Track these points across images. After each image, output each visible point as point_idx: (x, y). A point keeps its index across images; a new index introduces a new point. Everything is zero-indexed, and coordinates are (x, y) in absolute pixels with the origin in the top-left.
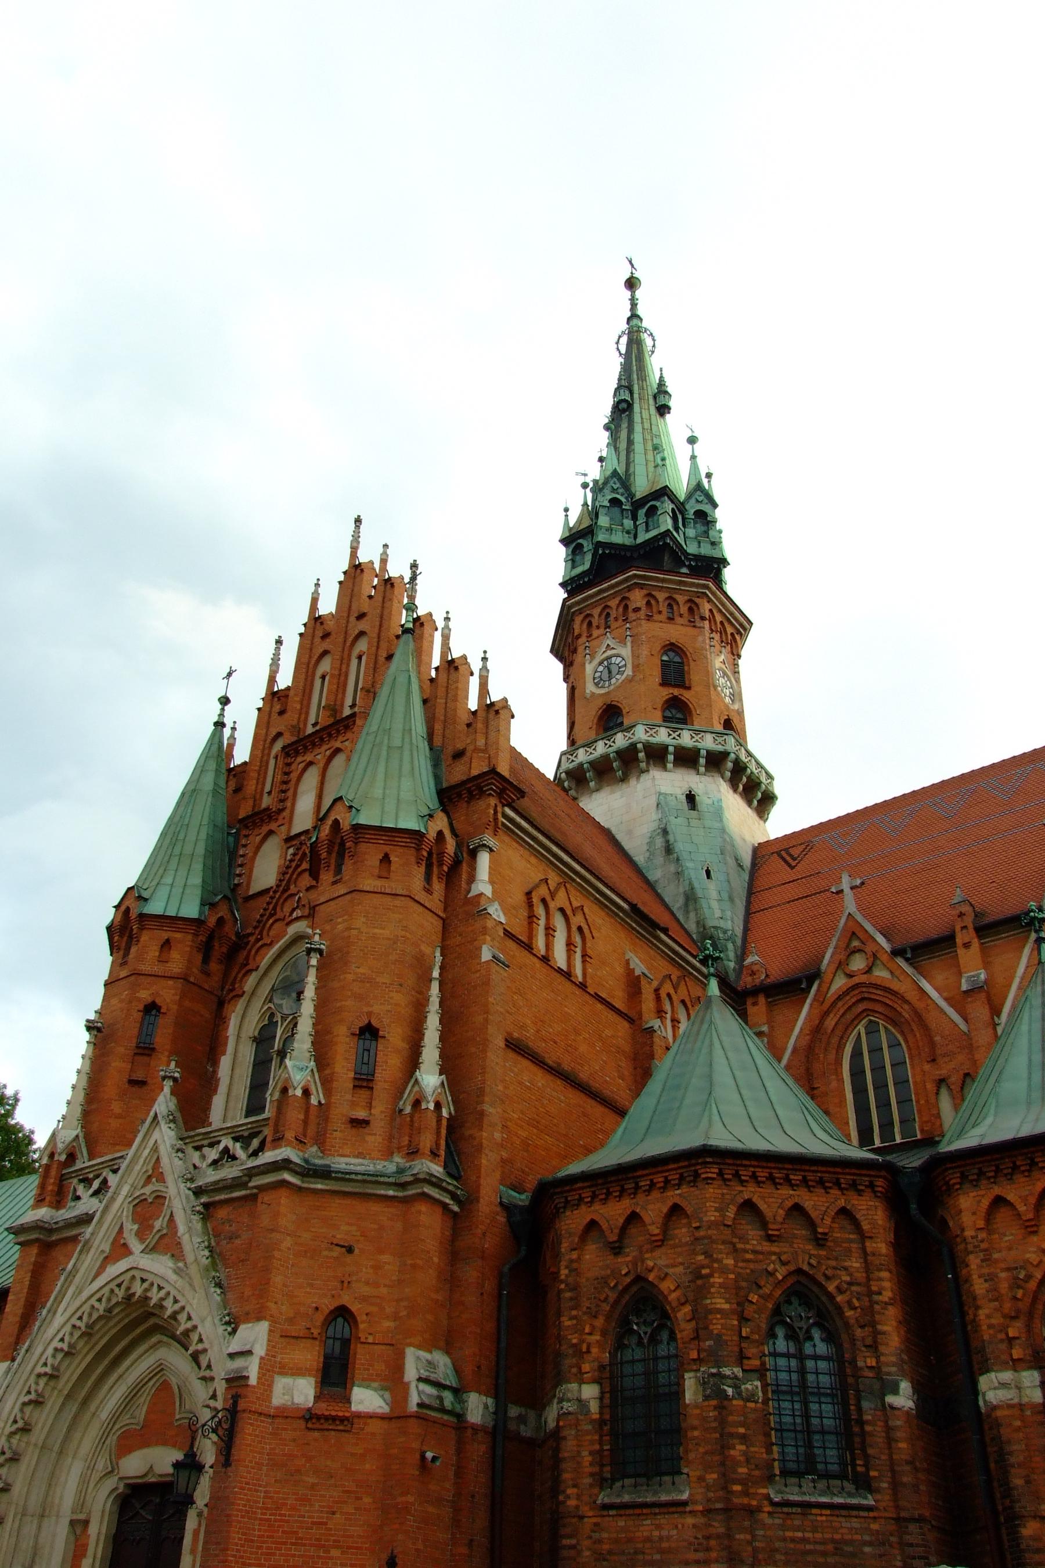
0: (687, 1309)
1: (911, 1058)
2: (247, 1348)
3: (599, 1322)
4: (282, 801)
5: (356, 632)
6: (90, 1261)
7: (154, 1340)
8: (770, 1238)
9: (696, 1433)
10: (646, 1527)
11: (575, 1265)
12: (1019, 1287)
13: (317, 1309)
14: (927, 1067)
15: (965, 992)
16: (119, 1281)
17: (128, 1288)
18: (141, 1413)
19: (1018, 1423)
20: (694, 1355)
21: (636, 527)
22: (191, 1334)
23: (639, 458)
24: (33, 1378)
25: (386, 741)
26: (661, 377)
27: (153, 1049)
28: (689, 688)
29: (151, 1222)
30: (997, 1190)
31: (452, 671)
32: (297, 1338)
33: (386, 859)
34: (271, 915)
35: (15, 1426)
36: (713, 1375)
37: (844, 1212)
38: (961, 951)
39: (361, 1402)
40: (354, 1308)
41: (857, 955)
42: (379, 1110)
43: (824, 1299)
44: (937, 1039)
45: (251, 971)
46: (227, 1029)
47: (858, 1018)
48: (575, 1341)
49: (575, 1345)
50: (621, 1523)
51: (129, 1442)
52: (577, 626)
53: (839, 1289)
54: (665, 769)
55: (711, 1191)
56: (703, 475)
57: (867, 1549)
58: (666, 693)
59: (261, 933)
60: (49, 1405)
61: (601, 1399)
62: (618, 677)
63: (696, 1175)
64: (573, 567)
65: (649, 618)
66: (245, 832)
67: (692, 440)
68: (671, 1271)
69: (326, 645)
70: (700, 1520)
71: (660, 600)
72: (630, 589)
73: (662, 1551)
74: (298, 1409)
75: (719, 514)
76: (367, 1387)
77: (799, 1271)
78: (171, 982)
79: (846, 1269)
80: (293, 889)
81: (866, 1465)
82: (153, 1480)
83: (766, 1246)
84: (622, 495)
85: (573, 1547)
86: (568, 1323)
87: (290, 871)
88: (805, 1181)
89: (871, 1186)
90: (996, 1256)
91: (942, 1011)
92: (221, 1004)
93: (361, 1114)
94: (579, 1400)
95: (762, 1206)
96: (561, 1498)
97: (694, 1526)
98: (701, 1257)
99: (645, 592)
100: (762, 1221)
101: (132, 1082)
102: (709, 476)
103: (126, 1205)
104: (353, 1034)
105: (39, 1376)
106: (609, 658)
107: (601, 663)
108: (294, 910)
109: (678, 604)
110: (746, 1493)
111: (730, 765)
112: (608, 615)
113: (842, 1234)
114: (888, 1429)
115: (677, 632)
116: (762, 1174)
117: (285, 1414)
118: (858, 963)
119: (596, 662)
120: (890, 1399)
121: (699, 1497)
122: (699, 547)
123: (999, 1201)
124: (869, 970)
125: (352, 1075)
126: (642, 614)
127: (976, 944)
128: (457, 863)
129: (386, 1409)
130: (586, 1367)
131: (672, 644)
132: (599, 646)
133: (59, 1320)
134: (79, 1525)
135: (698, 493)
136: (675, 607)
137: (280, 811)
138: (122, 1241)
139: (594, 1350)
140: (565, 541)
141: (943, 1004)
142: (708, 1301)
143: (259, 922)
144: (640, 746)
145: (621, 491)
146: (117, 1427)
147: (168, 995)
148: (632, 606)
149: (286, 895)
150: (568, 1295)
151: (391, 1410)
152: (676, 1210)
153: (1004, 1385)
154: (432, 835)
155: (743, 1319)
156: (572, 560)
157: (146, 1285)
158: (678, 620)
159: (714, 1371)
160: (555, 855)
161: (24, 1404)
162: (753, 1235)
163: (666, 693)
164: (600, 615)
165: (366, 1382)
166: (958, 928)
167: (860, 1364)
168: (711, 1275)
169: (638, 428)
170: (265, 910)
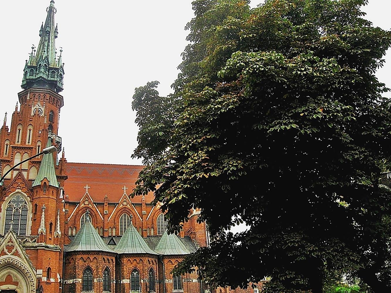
20: (96, 277)
67: (61, 51)
72: (47, 93)
83: (104, 263)
102: (63, 64)
139: (81, 275)
145: (47, 62)
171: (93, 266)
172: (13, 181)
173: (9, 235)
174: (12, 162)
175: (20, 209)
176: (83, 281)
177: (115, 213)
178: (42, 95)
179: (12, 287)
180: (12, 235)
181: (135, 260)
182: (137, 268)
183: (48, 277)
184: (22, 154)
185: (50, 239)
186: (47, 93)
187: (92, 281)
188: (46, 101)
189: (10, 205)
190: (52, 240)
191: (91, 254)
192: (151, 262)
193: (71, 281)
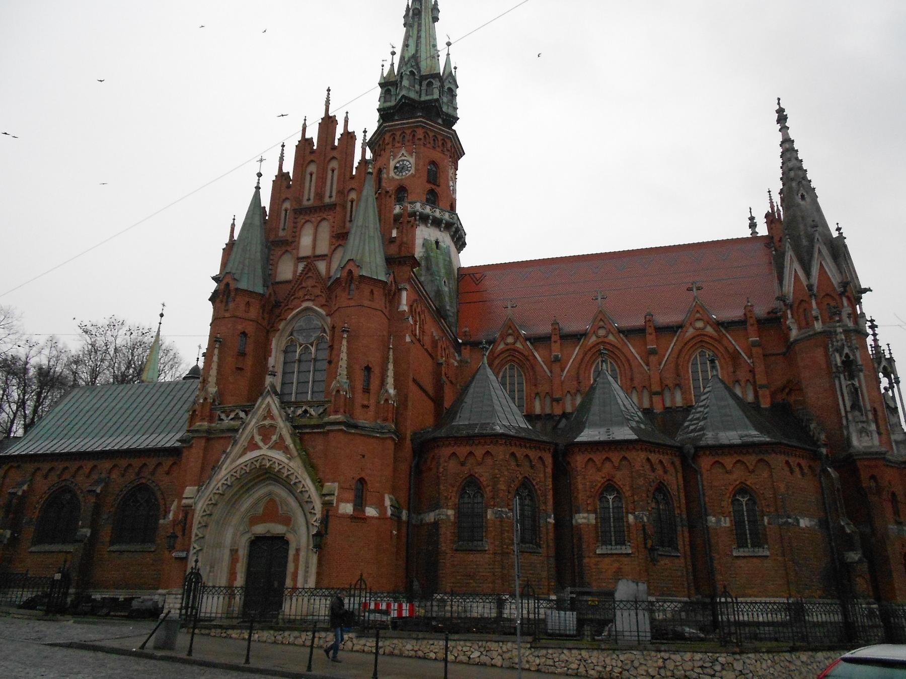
1: (526, 382)
2: (332, 492)
3: (455, 489)
4: (293, 237)
5: (331, 156)
6: (238, 449)
7: (268, 482)
8: (518, 465)
9: (491, 529)
10: (471, 557)
11: (446, 468)
12: (593, 488)
17: (261, 463)
19: (587, 529)
20: (492, 503)
23: (423, 47)
25: (367, 233)
28: (439, 186)
29: (269, 436)
30: (591, 456)
31: (388, 197)
33: (372, 292)
34: (293, 295)
35: (205, 514)
37: (540, 458)
38: (553, 344)
40: (366, 479)
41: (510, 336)
42: (372, 401)
44: (538, 377)
45: (282, 320)
52: (387, 137)
53: (536, 483)
54: (427, 226)
55: (502, 448)
56: (452, 67)
58: (429, 186)
62: (407, 172)
64: (385, 102)
65: (424, 145)
66: (273, 248)
67: (449, 44)
69: (312, 157)
70: (491, 556)
72: (417, 127)
73: (477, 565)
74: (348, 515)
75: (458, 91)
76: (371, 507)
77: (526, 477)
78: (251, 323)
80: (304, 285)
81: (540, 540)
83: (517, 468)
84: (415, 69)
87: (303, 275)
90: (587, 477)
92: (268, 332)
93: (366, 403)
94: (447, 515)
96: (439, 547)
102: (455, 68)
106: (403, 161)
107: (398, 162)
108: (305, 295)
110: (507, 548)
111: (454, 229)
113: (539, 465)
114: (547, 529)
116: (518, 443)
117: (344, 516)
118: (510, 340)
119: (396, 161)
120: (548, 520)
121: (491, 549)
122: (448, 109)
125: (362, 387)
128: (395, 294)
129: (377, 515)
130: (450, 504)
131: (433, 161)
132: (398, 153)
133: (223, 472)
134: (234, 552)
135: (450, 77)
136: (436, 141)
137: (292, 242)
139: (453, 498)
140: (381, 85)
141: (542, 363)
144: (418, 213)
145: (415, 67)
146: (249, 514)
147: (250, 329)
149: (300, 287)
151: (379, 514)
152: (488, 453)
153: (584, 518)
154: (389, 283)
155: (509, 492)
157: (271, 463)
160: (418, 288)
161: (208, 504)
162: (513, 463)
163: (429, 186)
164: (400, 136)
165: (370, 506)
167: (541, 508)
169: (423, 28)
171: (484, 474)
172: (295, 284)
173: (266, 402)
174: (295, 243)
175: (312, 346)
176: (459, 514)
177: (580, 357)
178: (408, 132)
179: (278, 529)
181: (607, 459)
182: (615, 482)
183: (359, 504)
184: (315, 224)
185: (365, 407)
186: (417, 127)
187: (483, 515)
188: (417, 142)
189: (292, 341)
190: (372, 408)
191: (476, 442)
192: (658, 467)
193: (430, 517)
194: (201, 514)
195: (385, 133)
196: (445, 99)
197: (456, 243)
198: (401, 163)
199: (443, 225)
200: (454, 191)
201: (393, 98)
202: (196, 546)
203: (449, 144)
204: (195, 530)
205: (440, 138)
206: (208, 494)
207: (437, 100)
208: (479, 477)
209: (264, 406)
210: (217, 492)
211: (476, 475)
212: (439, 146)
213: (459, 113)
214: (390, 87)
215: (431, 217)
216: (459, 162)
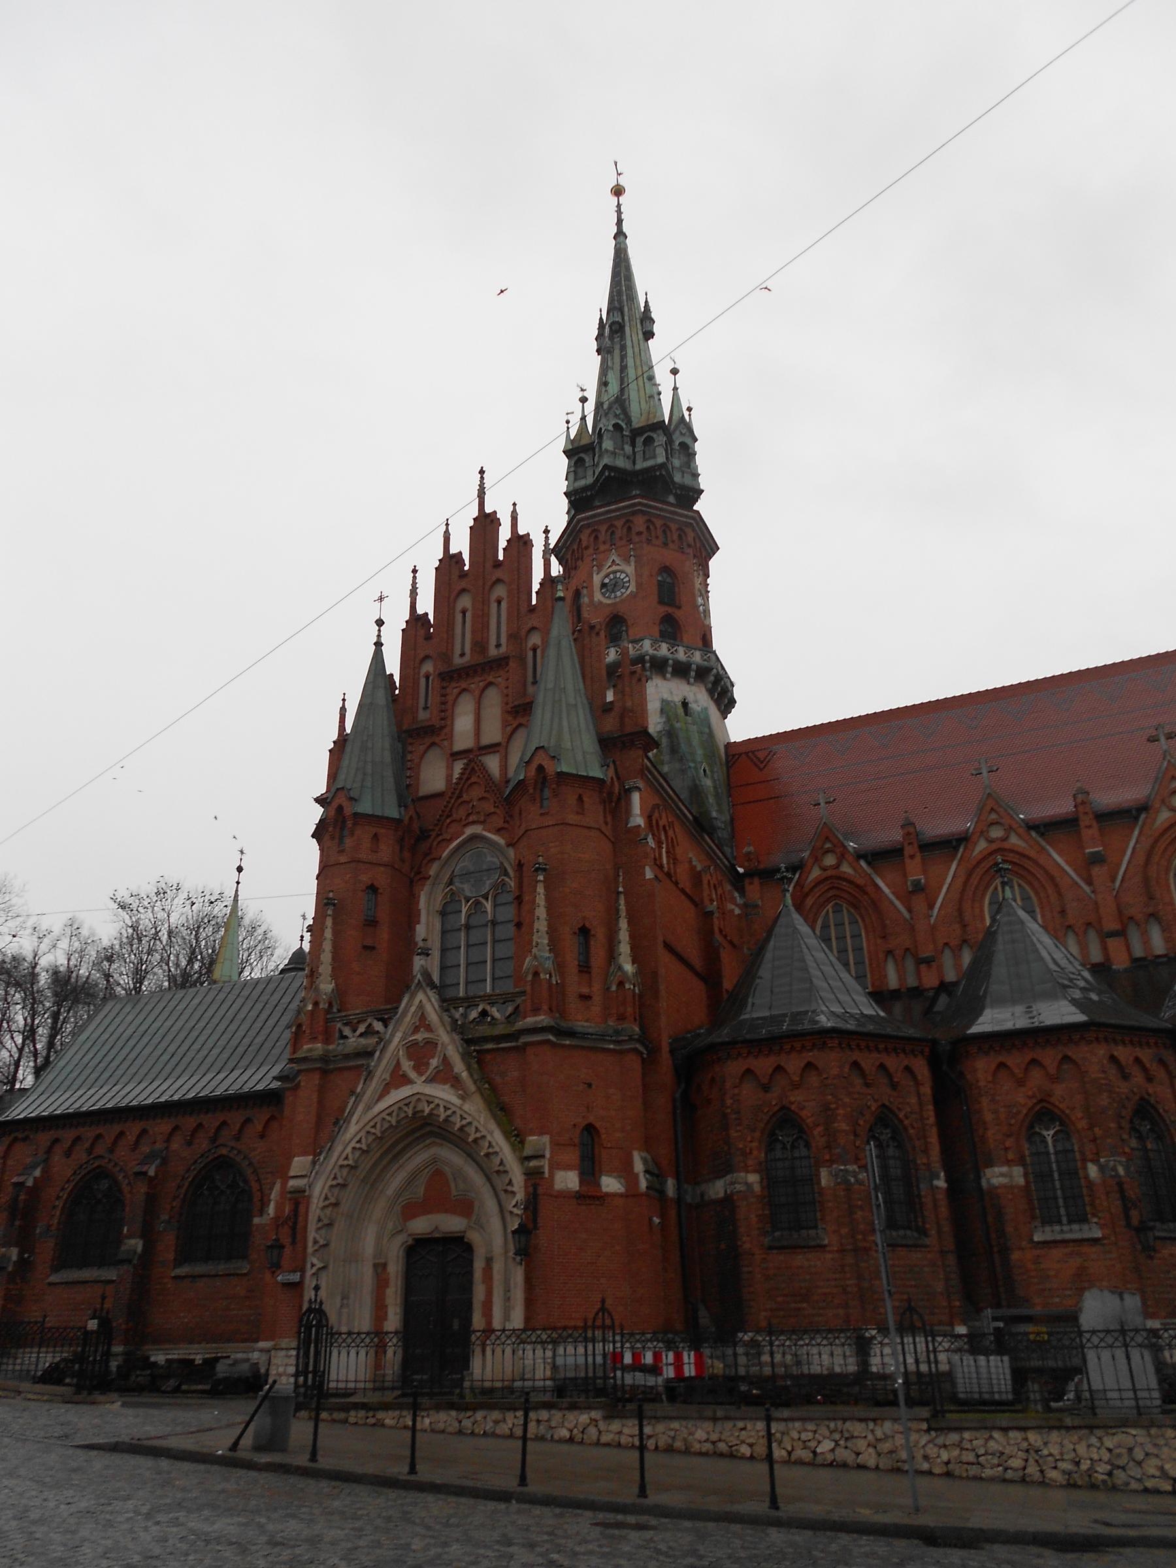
0: (820, 1129)
2: (541, 1153)
3: (757, 1134)
4: (442, 719)
5: (494, 579)
6: (375, 1084)
8: (867, 1085)
9: (830, 1204)
10: (799, 1260)
13: (575, 1125)
14: (879, 941)
15: (910, 892)
16: (407, 1101)
17: (415, 1107)
18: (421, 1191)
19: (1010, 1197)
20: (827, 1157)
21: (634, 453)
22: (480, 1142)
24: (337, 1168)
25: (563, 699)
26: (646, 302)
27: (377, 922)
28: (679, 608)
30: (1001, 1059)
31: (593, 635)
32: (564, 1145)
33: (580, 799)
34: (448, 816)
35: (327, 1203)
36: (842, 1170)
38: (908, 861)
39: (608, 1186)
40: (597, 1125)
42: (597, 987)
43: (896, 1122)
44: (888, 922)
45: (434, 859)
46: (418, 903)
47: (828, 901)
48: (741, 1146)
49: (741, 1149)
50: (782, 1257)
51: (411, 1210)
52: (584, 537)
54: (664, 678)
57: (926, 1269)
58: (663, 610)
59: (440, 830)
60: (350, 1187)
61: (761, 1182)
63: (825, 1043)
64: (575, 480)
65: (649, 541)
66: (410, 740)
67: (675, 372)
68: (806, 1104)
69: (464, 584)
71: (658, 526)
72: (634, 513)
77: (884, 1105)
78: (382, 869)
79: (908, 1103)
80: (465, 797)
81: (924, 1223)
82: (437, 1235)
85: (750, 1272)
86: (735, 1135)
88: (886, 1049)
89: (922, 1052)
91: (891, 902)
94: (746, 1183)
95: (863, 1064)
97: (832, 1259)
98: (830, 1097)
99: (646, 518)
100: (862, 1073)
101: (365, 948)
102: (689, 409)
103: (400, 1047)
104: (575, 933)
105: (341, 1166)
106: (615, 572)
107: (607, 576)
108: (468, 815)
109: (670, 530)
111: (712, 678)
112: (613, 533)
115: (669, 556)
116: (863, 1044)
117: (565, 1195)
118: (830, 860)
120: (936, 1183)
122: (683, 477)
123: (1002, 1065)
124: (837, 866)
126: (644, 537)
127: (918, 856)
128: (619, 799)
129: (622, 1190)
130: (750, 1162)
133: (353, 1128)
134: (380, 1268)
136: (668, 533)
137: (442, 728)
138: (401, 1073)
139: (755, 1153)
142: (836, 1125)
143: (438, 820)
144: (647, 658)
145: (622, 416)
146: (400, 1200)
147: (382, 878)
148: (635, 529)
150: (734, 1116)
151: (627, 1190)
152: (809, 1065)
153: (1002, 1175)
155: (856, 1135)
156: (574, 472)
157: (432, 1106)
158: (671, 546)
159: (842, 1168)
160: (660, 785)
161: (332, 1186)
162: (858, 1081)
163: (663, 610)
165: (609, 1173)
166: (906, 845)
167: (919, 1162)
168: (837, 1108)
169: (630, 351)
170: (443, 811)
171: (805, 1103)
172: (451, 798)
173: (416, 1002)
174: (446, 731)
175: (487, 899)
176: (770, 1182)
177: (960, 881)
178: (619, 523)
179: (452, 1223)
180: (425, 1001)
181: (1033, 1061)
182: (1053, 1105)
183: (590, 1171)
184: (477, 693)
185: (585, 998)
187: (814, 1179)
188: (636, 539)
189: (453, 893)
190: (597, 999)
193: (717, 1189)
194: (321, 1204)
195: (580, 531)
196: (676, 462)
197: (718, 702)
198: (612, 576)
199: (693, 674)
200: (707, 613)
201: (590, 472)
202: (315, 1261)
203: (691, 535)
204: (312, 1234)
205: (673, 527)
206: (330, 1168)
207: (662, 466)
208: (796, 1110)
209: (413, 1009)
210: (346, 1162)
211: (793, 1107)
212: (673, 542)
213: (703, 482)
214: (582, 455)
215: (671, 662)
216: (711, 563)
